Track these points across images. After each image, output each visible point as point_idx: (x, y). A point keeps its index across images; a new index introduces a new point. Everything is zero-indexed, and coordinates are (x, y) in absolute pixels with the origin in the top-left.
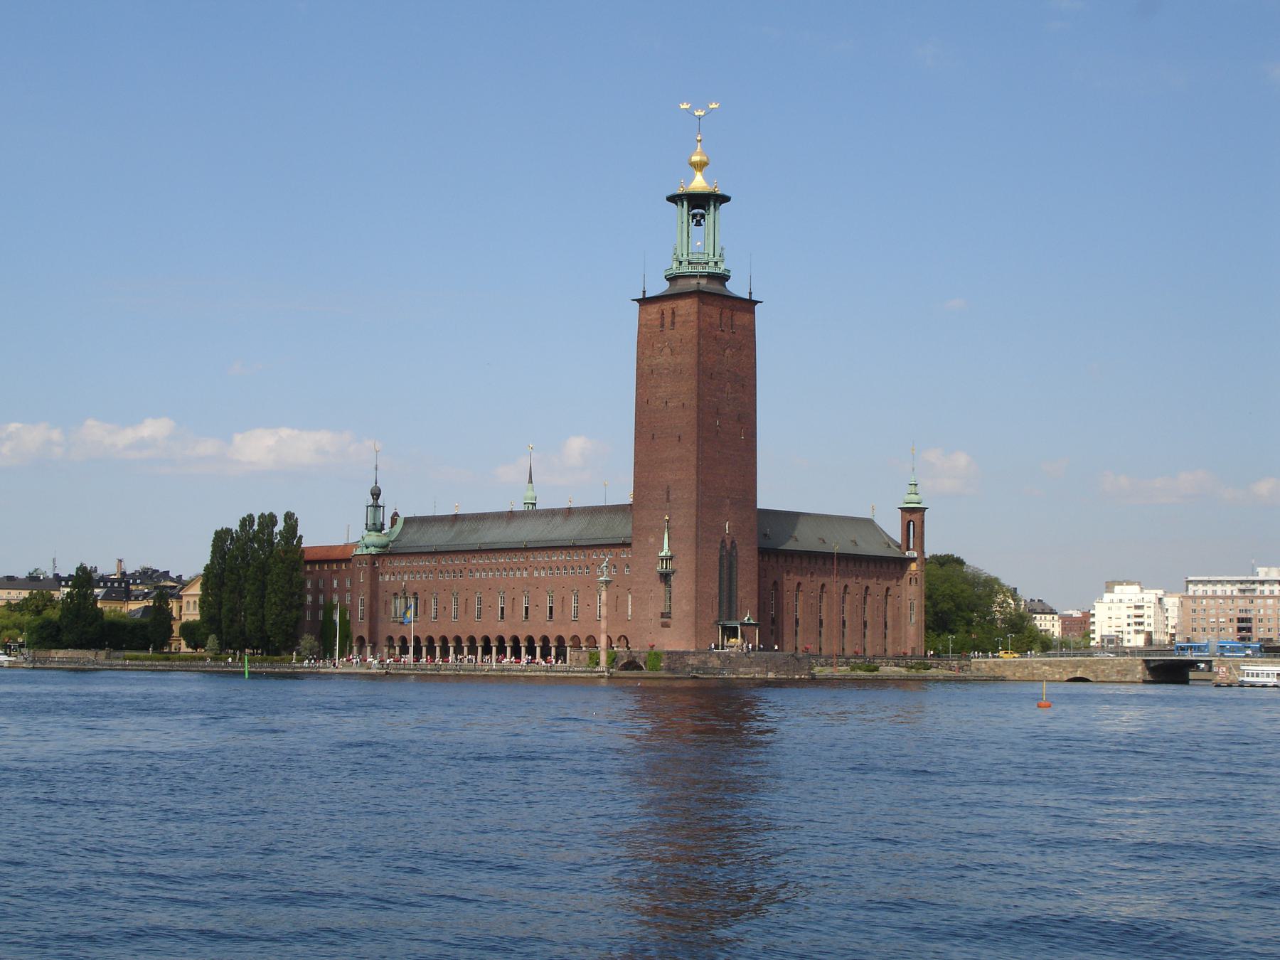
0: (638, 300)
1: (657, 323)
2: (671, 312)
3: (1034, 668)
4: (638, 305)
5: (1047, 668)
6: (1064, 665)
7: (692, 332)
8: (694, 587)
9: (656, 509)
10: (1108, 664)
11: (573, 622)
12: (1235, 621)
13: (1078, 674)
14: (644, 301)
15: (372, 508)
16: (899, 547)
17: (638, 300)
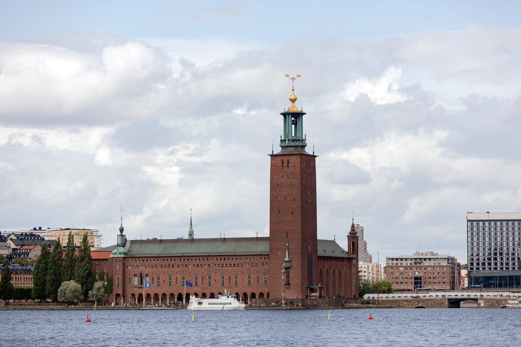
0: (270, 155)
1: (280, 165)
2: (287, 161)
3: (400, 303)
4: (270, 157)
5: (406, 303)
6: (413, 301)
7: (298, 170)
8: (301, 273)
9: (281, 241)
10: (433, 301)
11: (235, 287)
12: (413, 278)
13: (420, 305)
14: (273, 156)
15: (121, 236)
16: (347, 253)
17: (270, 155)
